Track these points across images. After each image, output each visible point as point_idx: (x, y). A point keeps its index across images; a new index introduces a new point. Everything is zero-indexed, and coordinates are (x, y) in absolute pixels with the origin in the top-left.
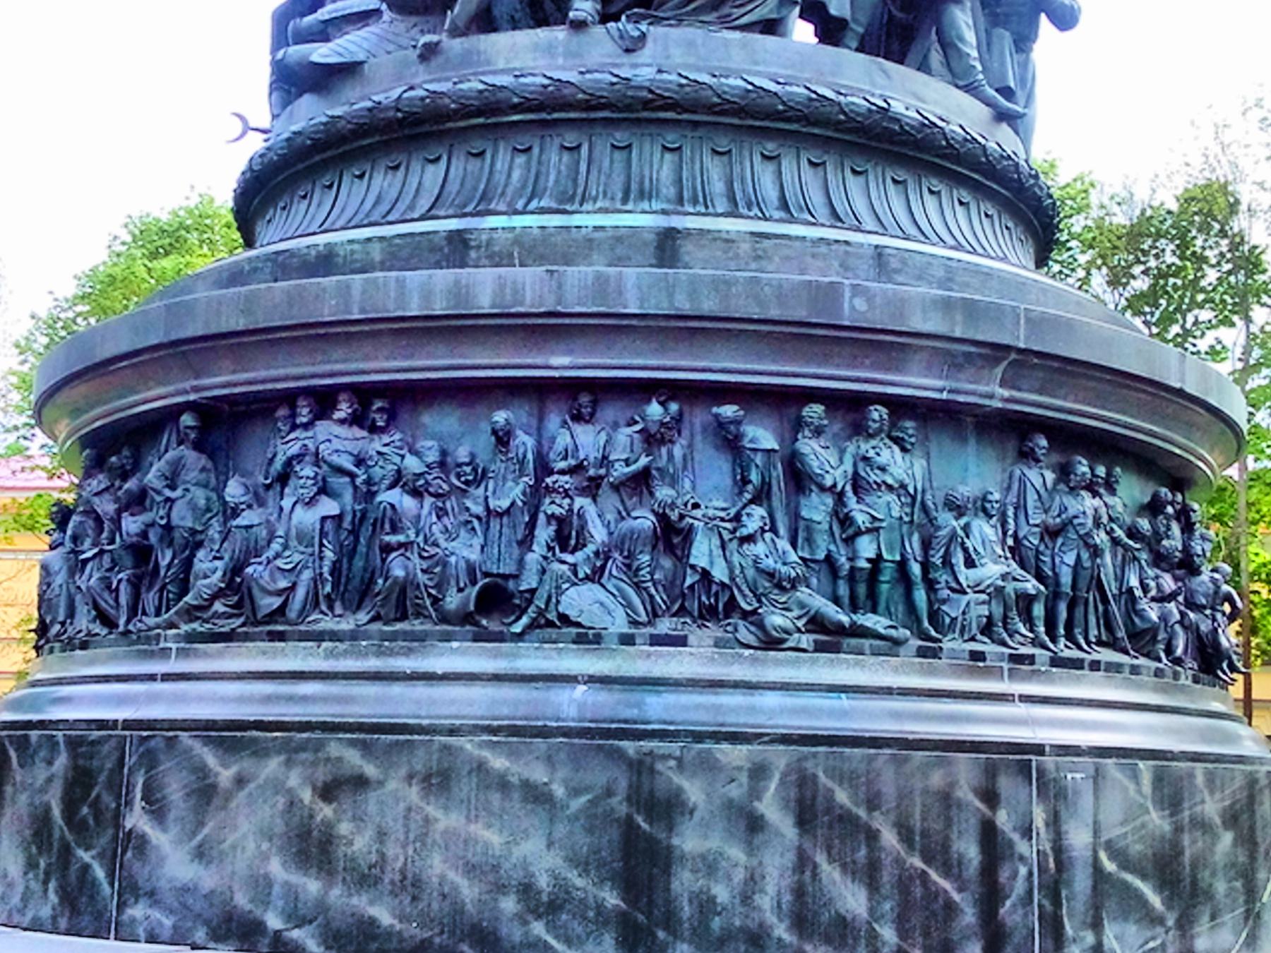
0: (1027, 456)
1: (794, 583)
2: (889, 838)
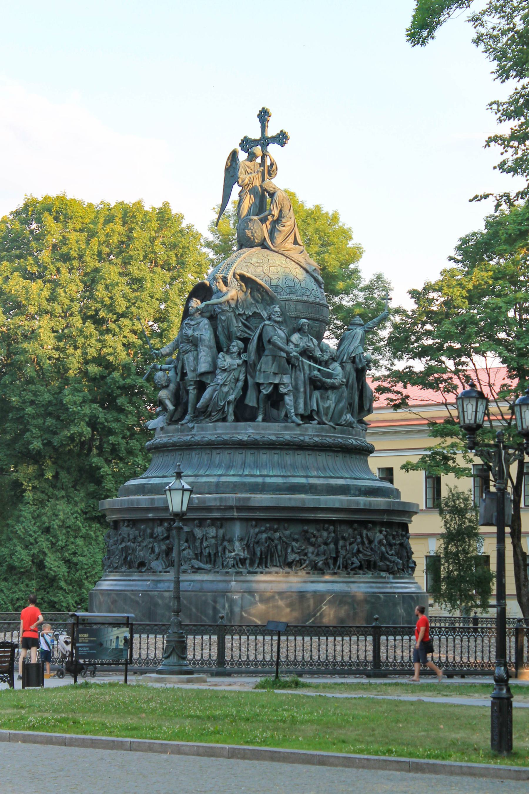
2: (194, 610)
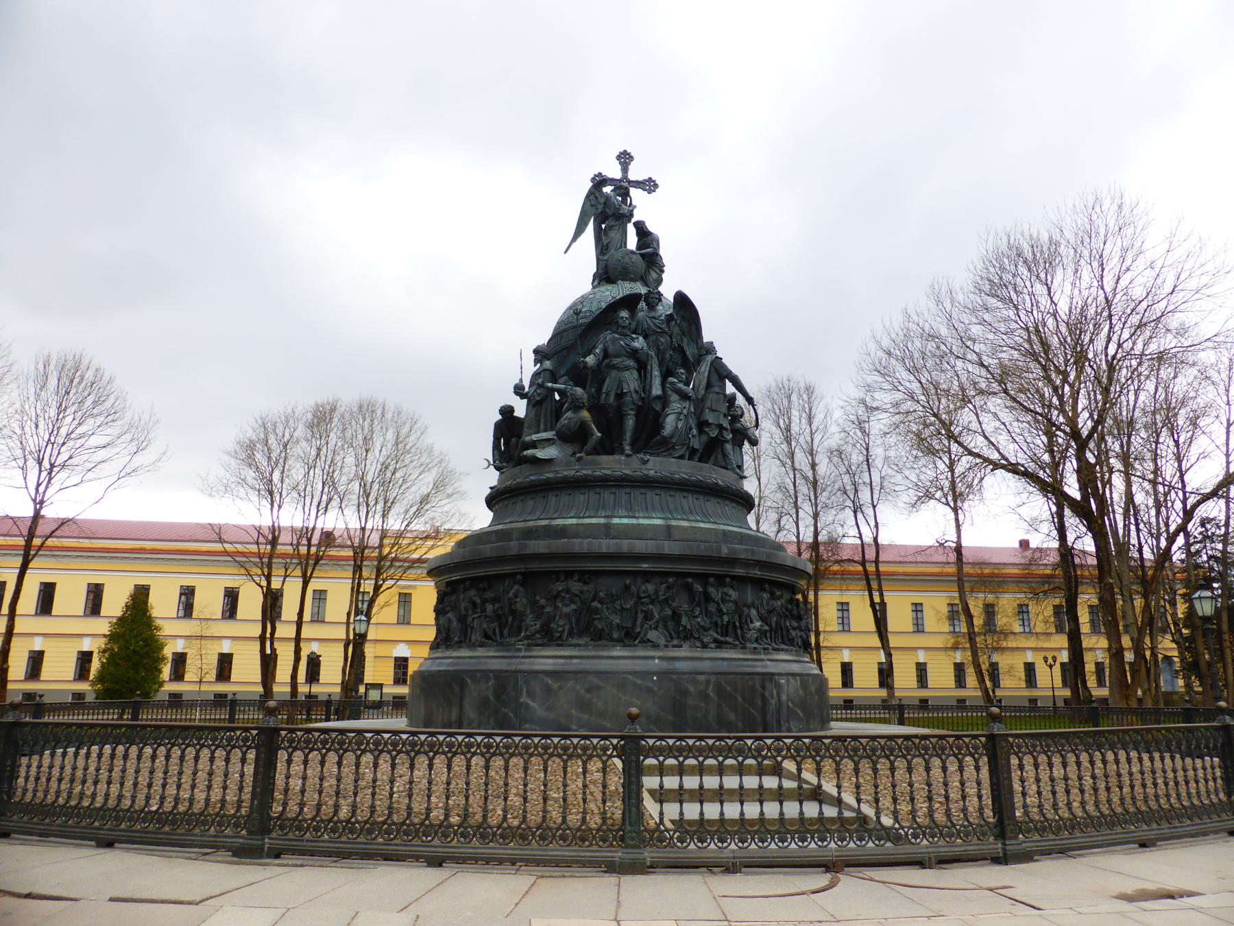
0: (763, 590)
1: (709, 629)
2: (740, 699)
